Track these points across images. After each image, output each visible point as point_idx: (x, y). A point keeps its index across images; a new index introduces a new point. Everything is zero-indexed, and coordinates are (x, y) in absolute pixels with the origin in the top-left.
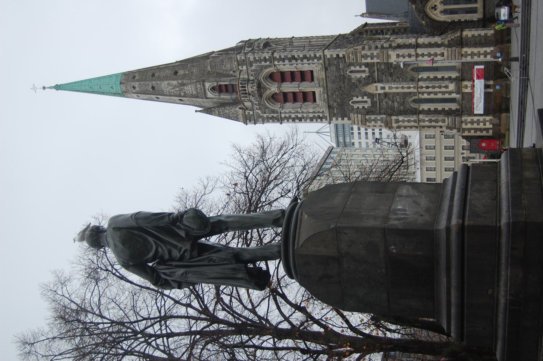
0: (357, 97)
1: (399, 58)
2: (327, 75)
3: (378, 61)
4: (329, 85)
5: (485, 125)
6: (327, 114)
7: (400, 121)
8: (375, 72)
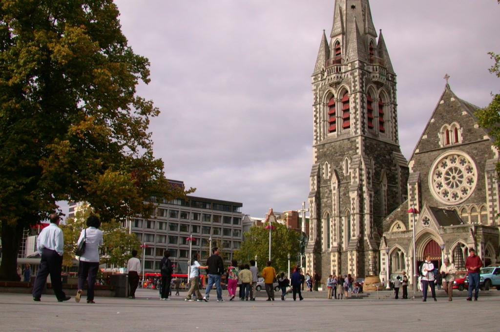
0: (330, 168)
2: (345, 141)
3: (352, 183)
4: (338, 143)
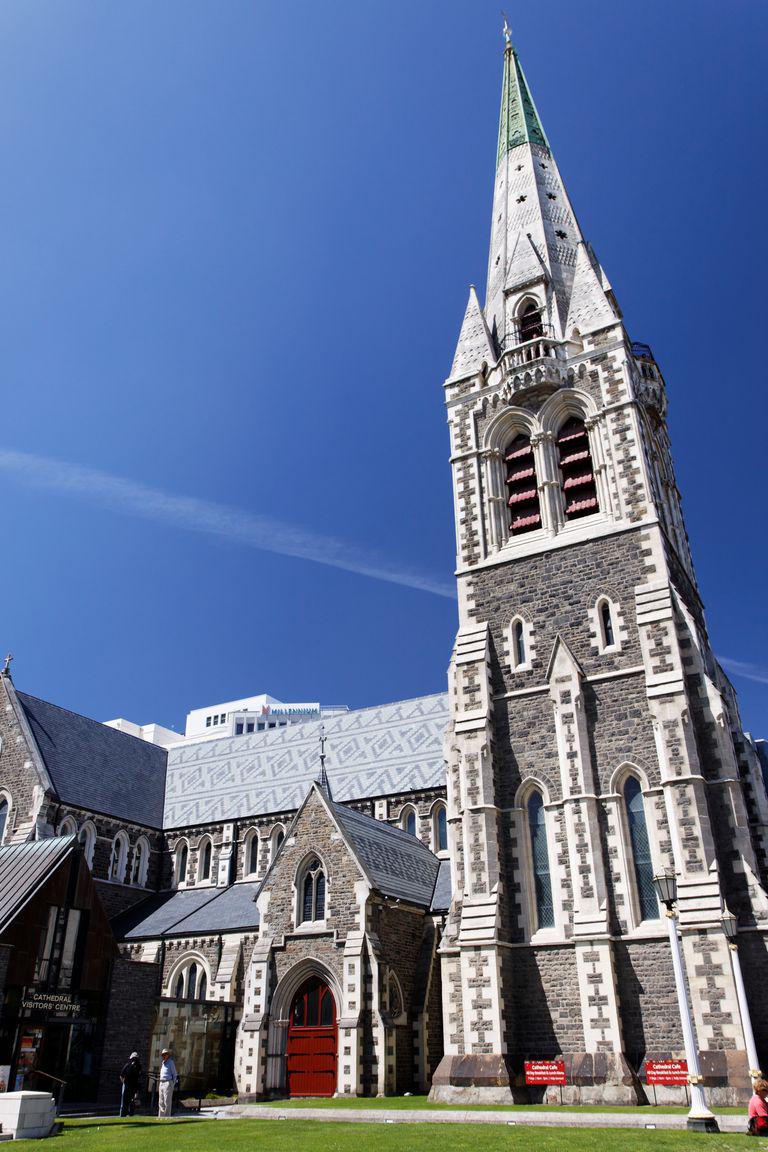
1: (665, 727)
3: (649, 672)
6: (482, 563)
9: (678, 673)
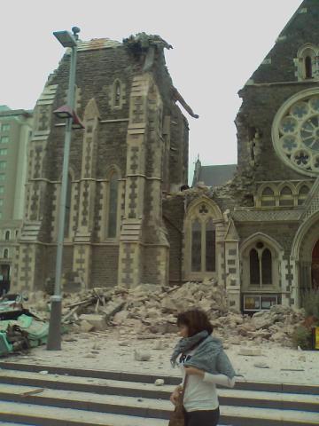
0: (81, 94)
5: (22, 279)
7: (38, 154)
8: (116, 118)
9: (143, 125)
